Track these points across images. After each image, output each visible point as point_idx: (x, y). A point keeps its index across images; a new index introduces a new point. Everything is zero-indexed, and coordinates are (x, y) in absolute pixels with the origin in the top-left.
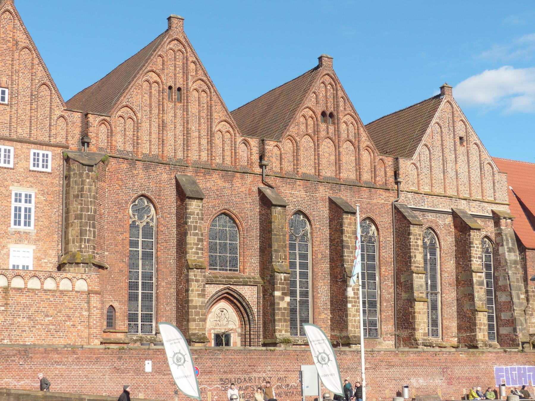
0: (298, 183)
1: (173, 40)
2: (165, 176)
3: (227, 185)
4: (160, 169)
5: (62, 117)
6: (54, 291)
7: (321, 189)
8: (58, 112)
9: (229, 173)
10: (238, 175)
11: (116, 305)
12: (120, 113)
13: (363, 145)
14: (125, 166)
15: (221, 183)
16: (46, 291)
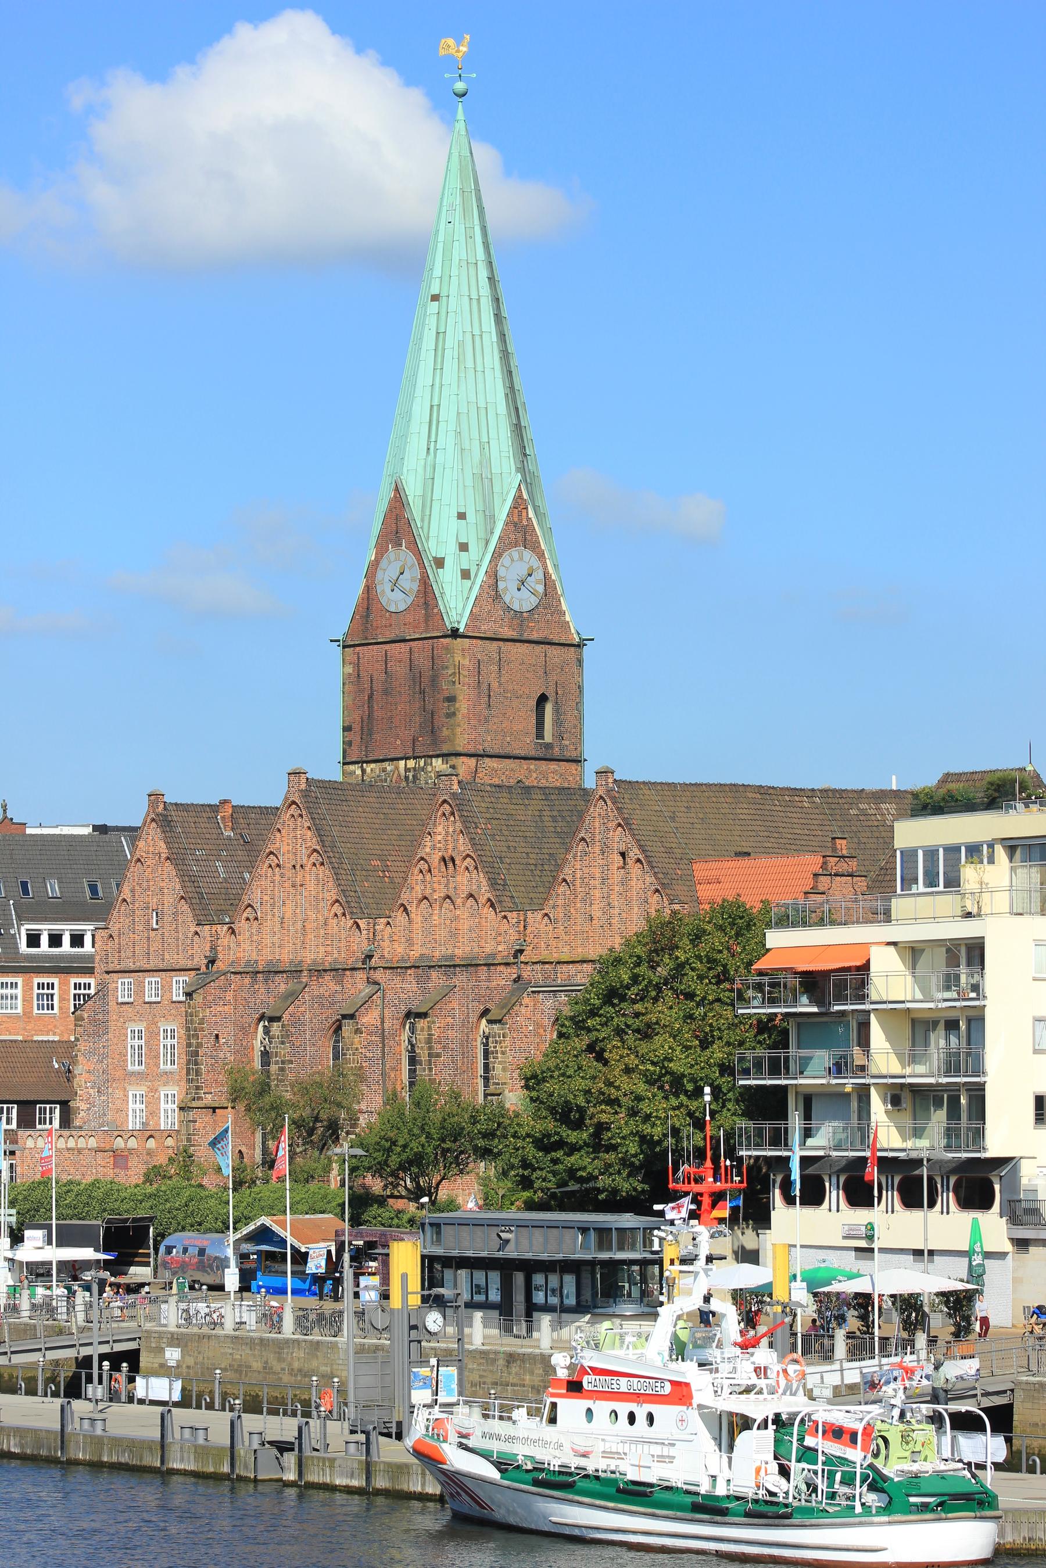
0: (409, 972)
1: (290, 806)
2: (283, 986)
3: (338, 988)
4: (278, 978)
5: (196, 933)
6: (73, 1149)
7: (434, 974)
8: (193, 929)
9: (338, 971)
10: (348, 973)
11: (244, 1149)
12: (245, 915)
13: (482, 900)
14: (247, 980)
15: (333, 986)
16: (68, 1149)
